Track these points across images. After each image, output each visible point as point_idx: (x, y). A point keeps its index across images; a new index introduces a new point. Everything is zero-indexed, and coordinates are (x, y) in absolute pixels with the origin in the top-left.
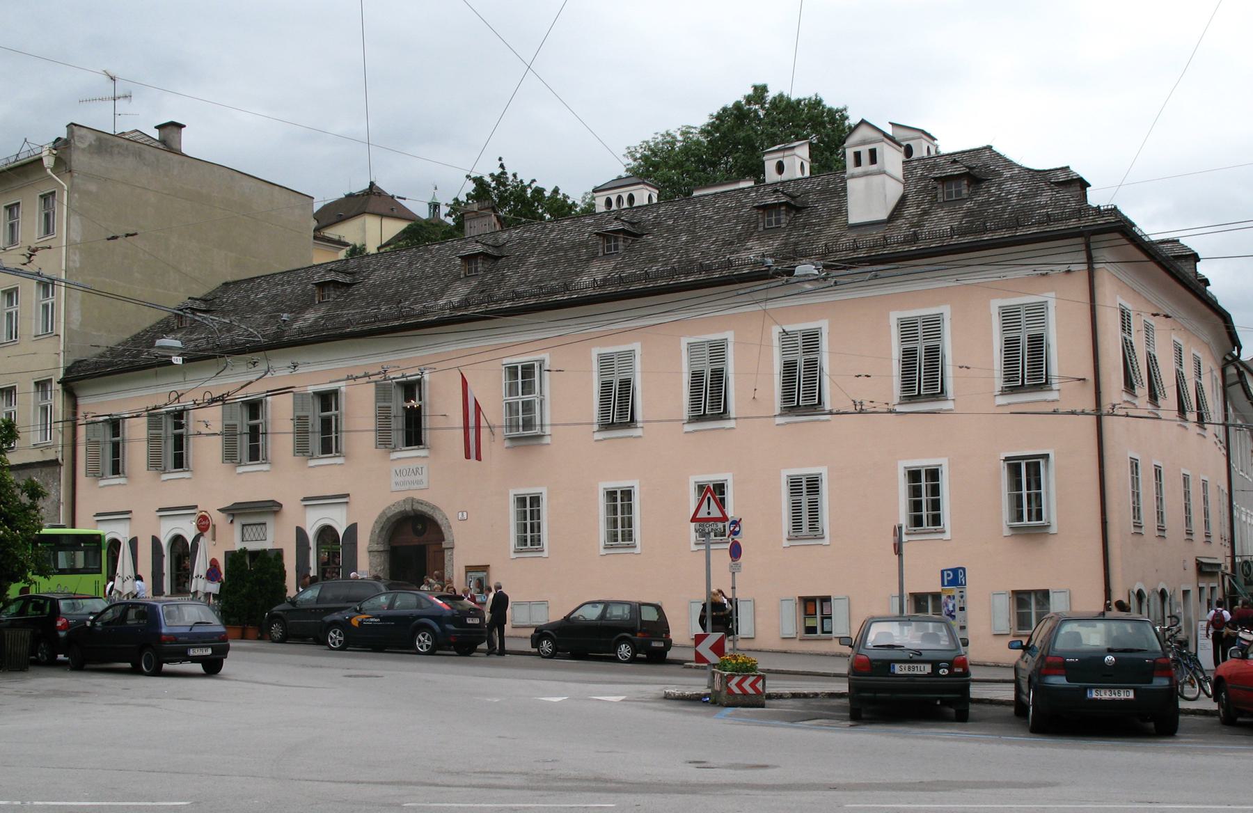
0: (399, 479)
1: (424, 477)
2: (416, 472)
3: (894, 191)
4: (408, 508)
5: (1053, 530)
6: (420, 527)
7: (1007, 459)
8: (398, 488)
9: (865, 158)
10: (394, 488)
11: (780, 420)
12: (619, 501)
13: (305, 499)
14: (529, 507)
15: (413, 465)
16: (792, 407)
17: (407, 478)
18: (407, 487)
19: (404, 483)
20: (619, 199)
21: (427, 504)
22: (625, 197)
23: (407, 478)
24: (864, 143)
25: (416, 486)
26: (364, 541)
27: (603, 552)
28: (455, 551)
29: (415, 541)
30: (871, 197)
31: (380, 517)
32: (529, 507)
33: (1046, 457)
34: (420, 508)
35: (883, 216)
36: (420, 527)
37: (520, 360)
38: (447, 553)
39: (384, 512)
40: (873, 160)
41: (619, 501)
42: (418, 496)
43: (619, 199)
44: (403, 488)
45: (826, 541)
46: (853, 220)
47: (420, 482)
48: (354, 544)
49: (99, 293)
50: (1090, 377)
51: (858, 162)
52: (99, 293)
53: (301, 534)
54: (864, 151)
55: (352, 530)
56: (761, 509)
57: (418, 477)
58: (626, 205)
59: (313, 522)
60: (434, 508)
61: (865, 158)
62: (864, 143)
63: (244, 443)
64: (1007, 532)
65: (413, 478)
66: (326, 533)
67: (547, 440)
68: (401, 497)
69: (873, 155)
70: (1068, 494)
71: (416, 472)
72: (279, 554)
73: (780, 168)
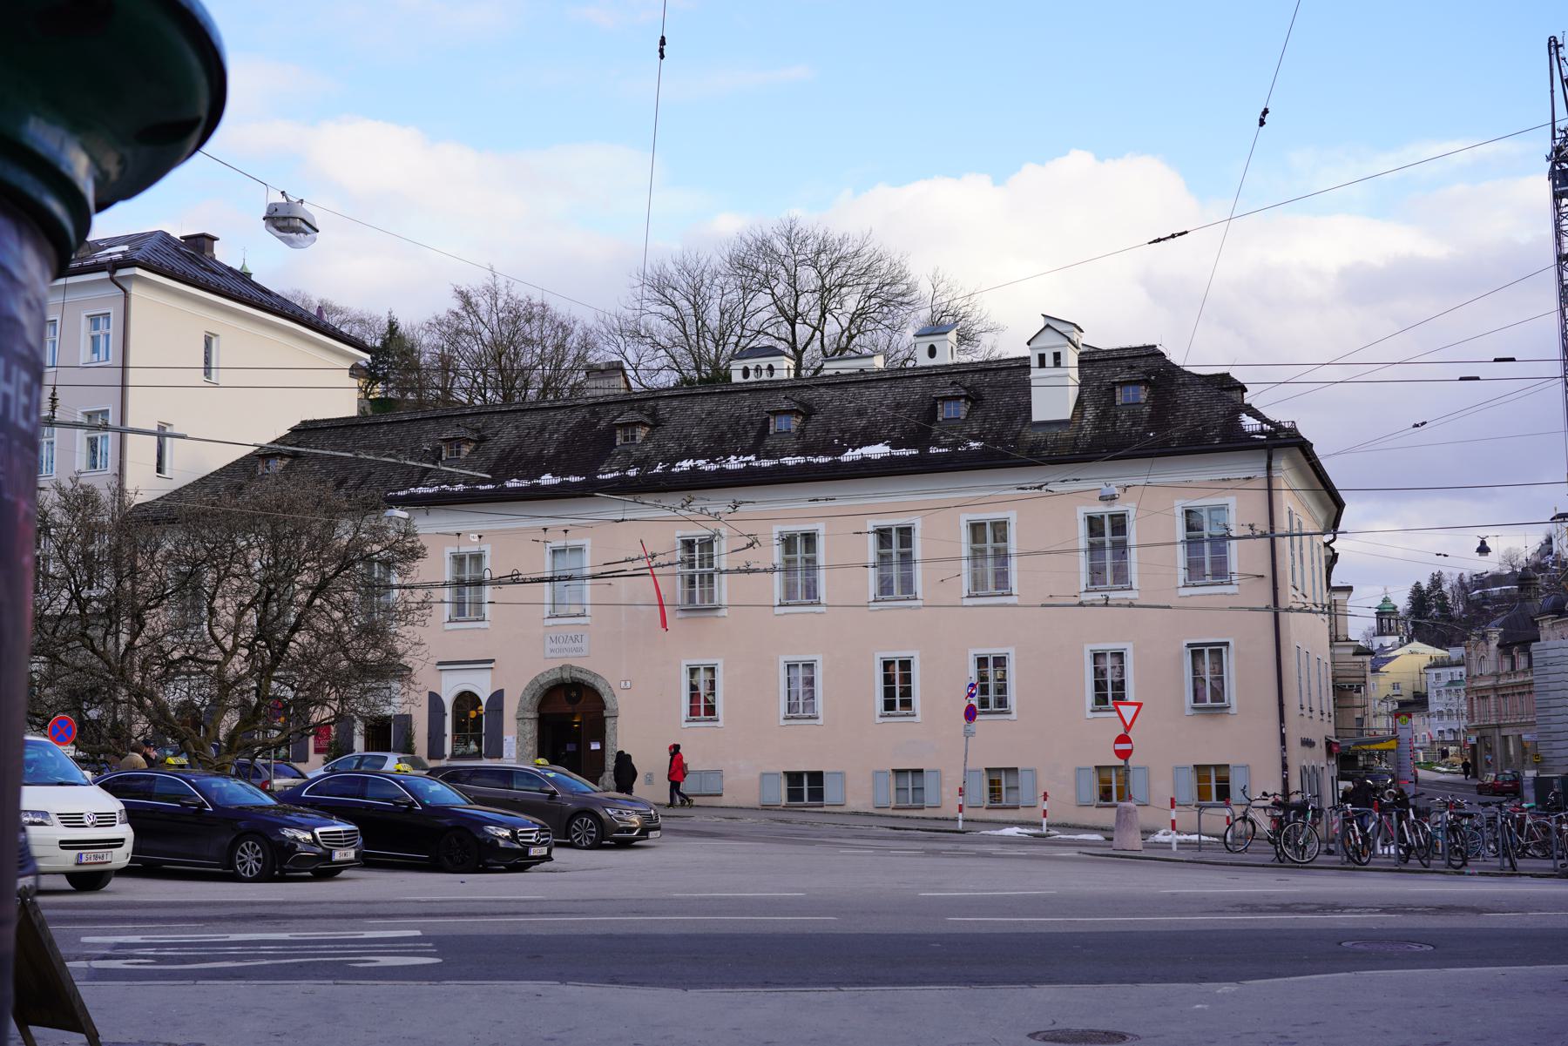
0: (554, 646)
2: (575, 639)
3: (1073, 393)
4: (566, 675)
5: (1233, 710)
6: (574, 694)
7: (1189, 645)
9: (1049, 361)
10: (549, 654)
13: (440, 663)
19: (560, 650)
21: (588, 672)
22: (764, 366)
26: (510, 708)
27: (783, 723)
30: (1054, 399)
31: (531, 684)
33: (1227, 644)
34: (578, 675)
35: (1068, 417)
36: (574, 694)
37: (697, 532)
38: (609, 722)
40: (1057, 363)
41: (803, 677)
42: (576, 664)
43: (758, 369)
45: (1014, 716)
46: (1036, 417)
47: (576, 650)
48: (501, 710)
49: (1028, 554)
50: (1268, 574)
51: (1042, 364)
52: (1028, 554)
53: (435, 701)
55: (497, 697)
56: (941, 687)
57: (577, 645)
59: (450, 687)
60: (596, 676)
61: (1049, 361)
64: (1189, 712)
65: (571, 645)
66: (466, 700)
67: (724, 612)
69: (1057, 356)
70: (1245, 677)
71: (575, 639)
72: (406, 720)
73: (932, 352)
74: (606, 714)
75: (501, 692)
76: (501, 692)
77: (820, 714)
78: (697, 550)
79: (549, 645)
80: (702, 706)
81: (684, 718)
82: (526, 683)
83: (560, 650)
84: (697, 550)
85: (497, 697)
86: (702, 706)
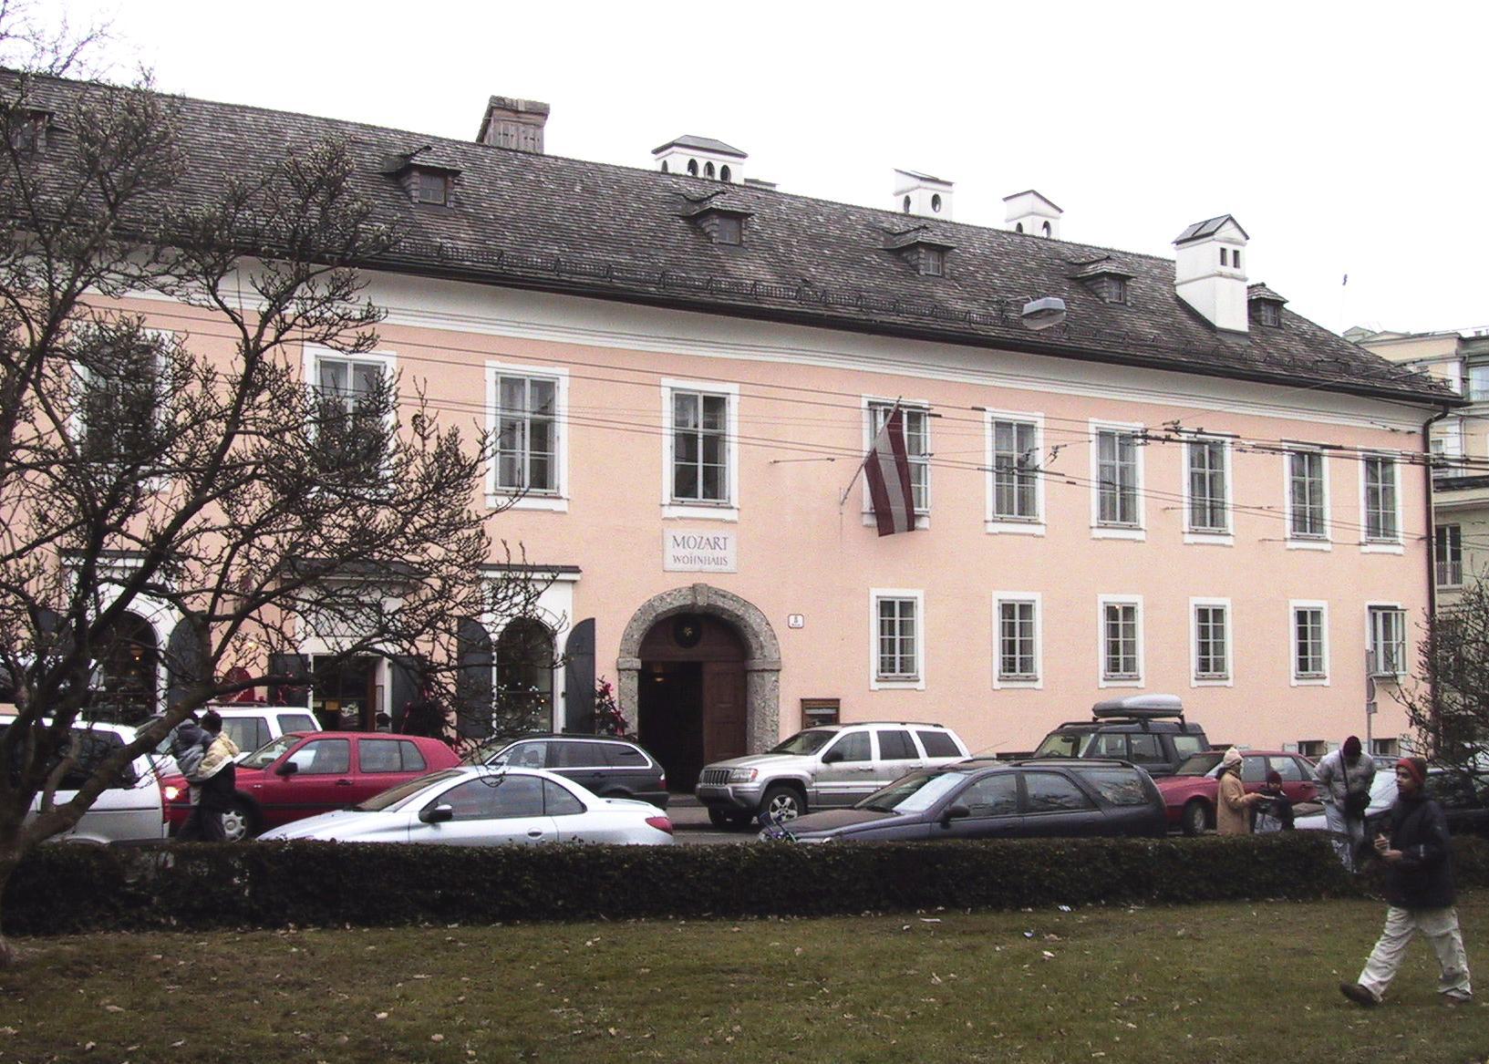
0: (681, 552)
1: (730, 553)
2: (715, 544)
4: (701, 601)
6: (688, 632)
8: (679, 566)
10: (670, 564)
11: (1190, 539)
12: (1016, 618)
14: (896, 616)
16: (684, 487)
17: (696, 552)
18: (697, 566)
19: (691, 560)
20: (710, 167)
23: (696, 552)
24: (1230, 241)
25: (713, 567)
29: (682, 654)
31: (643, 611)
32: (896, 616)
39: (650, 604)
43: (710, 167)
44: (688, 567)
47: (716, 561)
54: (1230, 249)
55: (584, 634)
57: (718, 553)
58: (718, 177)
60: (746, 604)
62: (1230, 241)
63: (524, 453)
65: (706, 552)
68: (687, 582)
71: (715, 544)
75: (592, 621)
76: (592, 621)
77: (1039, 675)
78: (900, 426)
80: (896, 655)
81: (874, 676)
82: (633, 609)
83: (691, 560)
84: (900, 426)
85: (584, 634)
86: (896, 655)
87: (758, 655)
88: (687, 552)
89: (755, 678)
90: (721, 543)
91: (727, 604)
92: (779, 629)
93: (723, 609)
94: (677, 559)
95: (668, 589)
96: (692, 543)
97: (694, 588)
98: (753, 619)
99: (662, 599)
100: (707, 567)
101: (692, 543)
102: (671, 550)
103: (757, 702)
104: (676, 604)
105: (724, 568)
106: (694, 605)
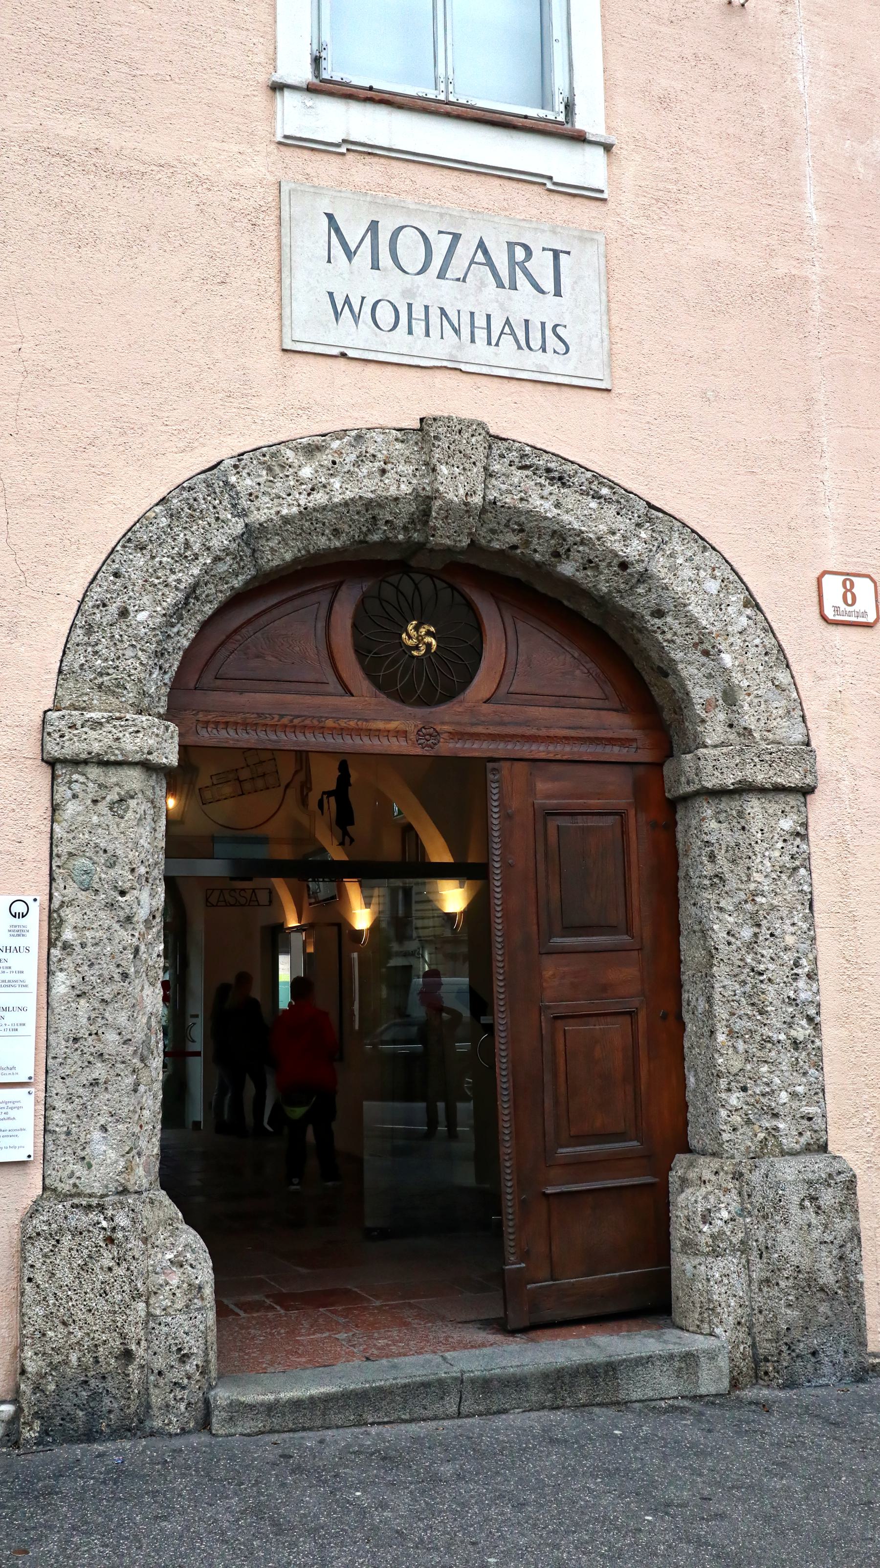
0: (360, 281)
1: (579, 310)
4: (456, 485)
6: (419, 637)
8: (356, 337)
10: (311, 324)
15: (498, 220)
17: (432, 291)
18: (439, 347)
19: (404, 318)
21: (598, 487)
23: (432, 291)
25: (506, 356)
28: (819, 809)
31: (180, 506)
34: (542, 502)
36: (419, 637)
44: (398, 344)
47: (522, 335)
57: (523, 303)
65: (482, 297)
74: (714, 760)
79: (315, 274)
82: (133, 494)
83: (404, 318)
87: (714, 730)
88: (385, 285)
89: (710, 825)
90: (541, 266)
91: (575, 513)
92: (795, 628)
93: (562, 539)
94: (340, 307)
95: (305, 428)
96: (411, 251)
97: (424, 433)
98: (681, 576)
99: (269, 458)
100: (479, 354)
101: (411, 251)
102: (315, 274)
103: (719, 920)
104: (341, 490)
105: (556, 366)
106: (425, 504)
